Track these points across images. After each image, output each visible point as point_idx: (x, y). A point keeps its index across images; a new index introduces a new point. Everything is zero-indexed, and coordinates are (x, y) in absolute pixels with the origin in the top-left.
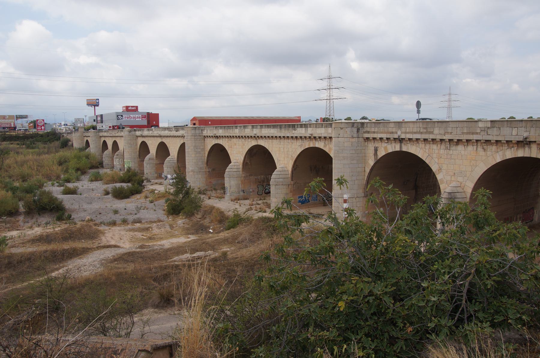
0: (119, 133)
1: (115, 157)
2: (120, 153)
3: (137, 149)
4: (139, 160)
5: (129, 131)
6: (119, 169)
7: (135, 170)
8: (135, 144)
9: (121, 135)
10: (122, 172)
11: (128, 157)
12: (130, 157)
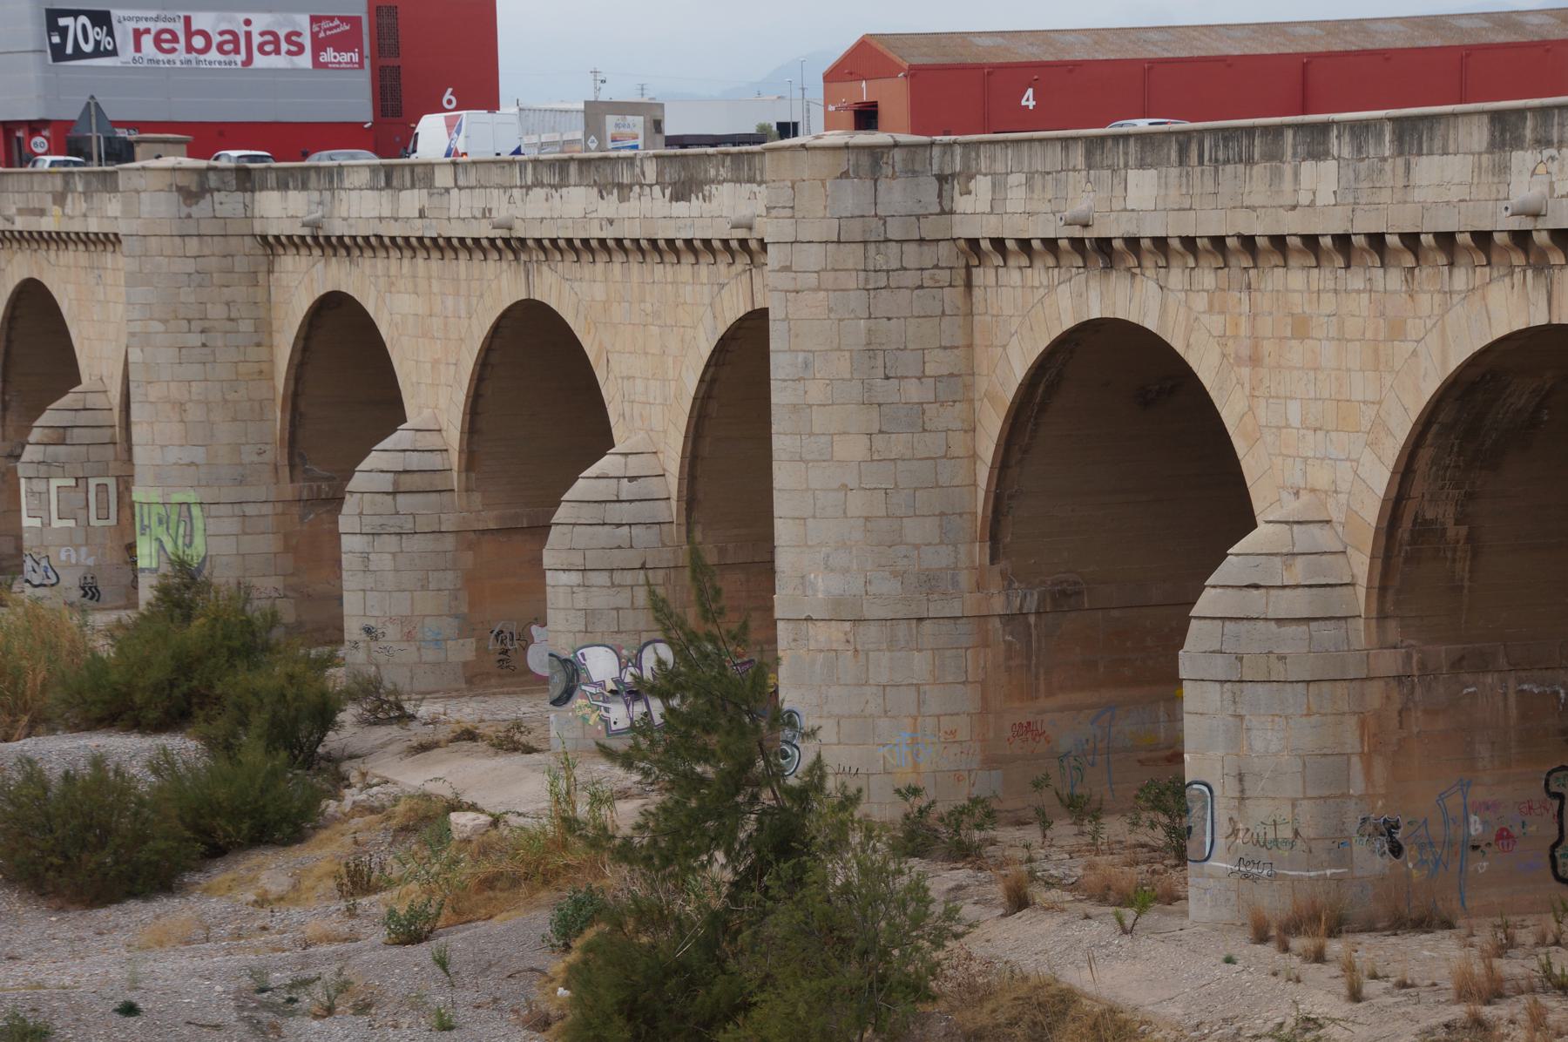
0: (75, 204)
1: (30, 453)
2: (83, 418)
3: (265, 375)
4: (288, 490)
5: (183, 180)
6: (71, 580)
7: (244, 591)
8: (246, 326)
9: (94, 226)
10: (101, 619)
11: (173, 455)
12: (199, 455)
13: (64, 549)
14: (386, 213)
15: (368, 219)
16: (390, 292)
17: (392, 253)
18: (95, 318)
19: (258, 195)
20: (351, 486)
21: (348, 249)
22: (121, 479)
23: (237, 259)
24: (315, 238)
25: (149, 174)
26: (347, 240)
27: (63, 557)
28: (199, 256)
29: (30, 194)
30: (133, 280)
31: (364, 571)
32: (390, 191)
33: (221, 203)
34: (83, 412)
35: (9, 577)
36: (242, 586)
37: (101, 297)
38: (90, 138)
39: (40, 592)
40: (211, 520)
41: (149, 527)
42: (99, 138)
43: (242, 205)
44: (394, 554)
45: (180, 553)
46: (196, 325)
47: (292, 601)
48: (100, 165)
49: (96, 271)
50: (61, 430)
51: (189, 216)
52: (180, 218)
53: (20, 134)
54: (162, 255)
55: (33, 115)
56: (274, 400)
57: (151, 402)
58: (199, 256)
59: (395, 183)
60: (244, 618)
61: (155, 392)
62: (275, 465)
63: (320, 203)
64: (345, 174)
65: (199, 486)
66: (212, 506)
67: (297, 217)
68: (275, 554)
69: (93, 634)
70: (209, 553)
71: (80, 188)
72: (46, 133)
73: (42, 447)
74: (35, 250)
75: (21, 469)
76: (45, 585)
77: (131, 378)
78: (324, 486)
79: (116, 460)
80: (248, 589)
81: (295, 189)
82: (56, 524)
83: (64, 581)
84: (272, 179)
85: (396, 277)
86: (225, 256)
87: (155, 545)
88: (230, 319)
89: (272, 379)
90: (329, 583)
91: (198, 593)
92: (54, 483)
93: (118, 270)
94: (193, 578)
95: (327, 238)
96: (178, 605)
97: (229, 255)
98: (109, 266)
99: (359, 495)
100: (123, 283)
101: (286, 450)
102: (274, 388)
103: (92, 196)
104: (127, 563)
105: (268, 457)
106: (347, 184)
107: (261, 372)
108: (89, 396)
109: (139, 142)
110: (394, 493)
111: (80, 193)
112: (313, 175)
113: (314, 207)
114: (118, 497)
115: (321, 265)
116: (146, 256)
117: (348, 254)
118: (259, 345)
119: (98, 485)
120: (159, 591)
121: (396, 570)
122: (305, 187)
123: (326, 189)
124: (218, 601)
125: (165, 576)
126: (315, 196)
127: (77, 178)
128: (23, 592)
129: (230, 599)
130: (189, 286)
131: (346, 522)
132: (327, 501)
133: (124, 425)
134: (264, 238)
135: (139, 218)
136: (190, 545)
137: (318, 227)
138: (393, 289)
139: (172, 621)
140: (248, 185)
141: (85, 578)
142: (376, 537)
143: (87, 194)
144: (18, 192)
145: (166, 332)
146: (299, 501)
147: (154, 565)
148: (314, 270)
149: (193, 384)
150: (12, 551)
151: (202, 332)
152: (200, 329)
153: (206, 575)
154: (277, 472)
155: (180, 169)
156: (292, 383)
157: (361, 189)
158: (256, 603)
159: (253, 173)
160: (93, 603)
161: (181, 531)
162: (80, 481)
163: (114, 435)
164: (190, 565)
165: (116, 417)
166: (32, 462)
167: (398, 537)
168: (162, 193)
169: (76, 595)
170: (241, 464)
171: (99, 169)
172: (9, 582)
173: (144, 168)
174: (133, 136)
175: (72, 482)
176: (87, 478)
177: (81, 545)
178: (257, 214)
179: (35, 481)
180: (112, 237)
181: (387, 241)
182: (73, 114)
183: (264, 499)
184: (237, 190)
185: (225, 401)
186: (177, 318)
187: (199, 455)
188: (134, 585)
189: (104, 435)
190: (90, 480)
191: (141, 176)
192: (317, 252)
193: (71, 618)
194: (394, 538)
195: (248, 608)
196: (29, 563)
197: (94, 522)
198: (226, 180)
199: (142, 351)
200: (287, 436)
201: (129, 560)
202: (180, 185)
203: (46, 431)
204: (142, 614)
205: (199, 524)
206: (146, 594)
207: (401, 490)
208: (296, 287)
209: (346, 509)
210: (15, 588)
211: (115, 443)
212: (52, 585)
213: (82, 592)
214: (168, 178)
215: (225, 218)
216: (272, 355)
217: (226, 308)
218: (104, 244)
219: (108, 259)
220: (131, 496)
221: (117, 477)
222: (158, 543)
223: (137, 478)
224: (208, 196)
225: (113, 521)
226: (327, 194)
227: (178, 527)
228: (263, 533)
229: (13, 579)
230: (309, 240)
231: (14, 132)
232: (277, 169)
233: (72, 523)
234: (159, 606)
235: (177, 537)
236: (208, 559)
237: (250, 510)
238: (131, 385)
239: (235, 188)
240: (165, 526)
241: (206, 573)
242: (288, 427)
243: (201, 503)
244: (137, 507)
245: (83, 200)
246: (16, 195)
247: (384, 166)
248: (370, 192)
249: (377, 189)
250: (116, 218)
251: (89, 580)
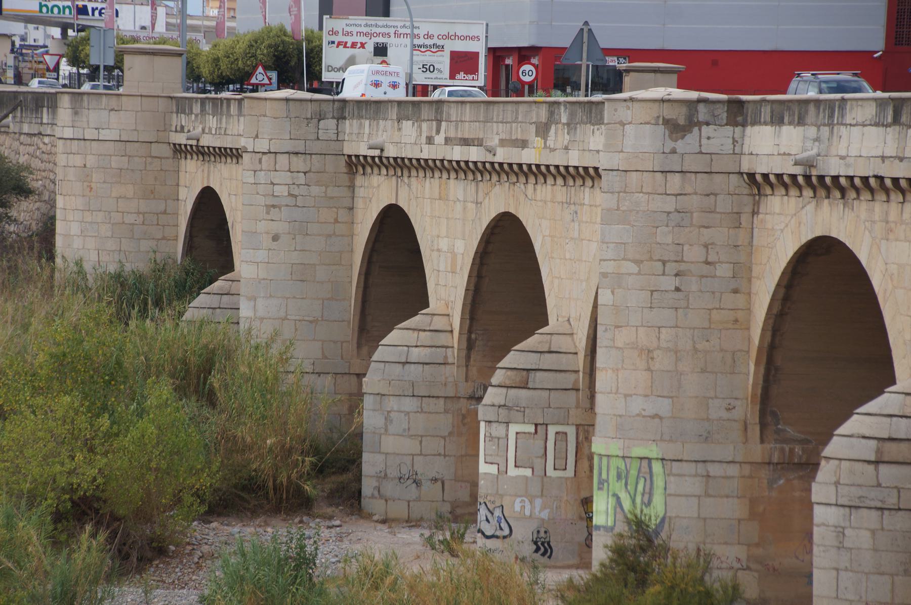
0: (558, 136)
1: (492, 396)
2: (548, 361)
3: (741, 324)
4: (757, 451)
5: (669, 112)
6: (523, 533)
7: (704, 559)
8: (724, 270)
9: (574, 158)
10: (552, 578)
11: (638, 405)
12: (664, 407)
13: (518, 500)
14: (890, 151)
15: (869, 158)
16: (887, 240)
17: (893, 196)
18: (568, 256)
19: (749, 130)
20: (828, 451)
21: (843, 191)
22: (581, 428)
23: (720, 197)
24: (808, 178)
25: (636, 105)
26: (843, 181)
27: (517, 508)
28: (681, 194)
29: (514, 125)
30: (610, 217)
31: (839, 548)
32: (897, 128)
33: (709, 138)
34: (547, 355)
35: (463, 525)
36: (702, 553)
37: (576, 235)
38: (581, 65)
39: (490, 544)
40: (672, 479)
41: (607, 481)
42: (588, 66)
43: (731, 141)
44: (873, 532)
45: (638, 512)
46: (671, 268)
47: (756, 575)
48: (586, 96)
49: (572, 207)
50: (525, 373)
51: (674, 151)
52: (664, 153)
53: (509, 61)
54: (641, 192)
55: (523, 41)
56: (748, 352)
57: (617, 348)
58: (681, 194)
59: (904, 119)
60: (702, 589)
61: (623, 337)
62: (745, 423)
63: (817, 139)
64: (848, 107)
65: (662, 440)
66: (674, 463)
67: (789, 154)
68: (739, 521)
69: (543, 593)
70: (668, 514)
71: (564, 119)
72: (535, 61)
73: (504, 390)
74: (514, 184)
75: (483, 412)
76: (497, 537)
77: (598, 322)
78: (798, 450)
79: (577, 407)
80: (709, 557)
81: (790, 124)
82: (513, 472)
83: (518, 534)
84: (766, 112)
85: (896, 223)
86: (708, 195)
87: (612, 501)
88: (707, 263)
89: (748, 329)
90: (797, 558)
91: (654, 557)
92: (514, 429)
93: (596, 206)
94: (650, 541)
95: (821, 178)
96: (632, 568)
97: (712, 194)
98: (586, 201)
99: (837, 462)
100: (599, 219)
101: (758, 407)
102: (749, 339)
103: (576, 129)
104: (581, 518)
105: (738, 413)
106: (848, 119)
107: (736, 321)
108: (555, 337)
109: (628, 71)
110: (877, 463)
111: (564, 124)
112: (812, 108)
113: (809, 144)
114: (577, 447)
115: (811, 207)
116: (625, 192)
117: (843, 196)
118: (736, 291)
119: (557, 433)
120: (613, 552)
121: (875, 550)
122: (801, 122)
123: (824, 125)
124: (675, 567)
125: (621, 536)
126: (812, 131)
127: (562, 108)
128: (475, 542)
129: (689, 566)
130: (667, 226)
131: (821, 490)
132: (800, 465)
133: (588, 370)
134: (752, 176)
135: (622, 151)
136: (649, 504)
137: (811, 166)
138: (891, 236)
139: (626, 586)
140: (740, 119)
141: (538, 532)
142: (853, 510)
143: (571, 126)
144: (502, 122)
145: (639, 273)
146: (769, 463)
147: (610, 523)
148: (804, 211)
149: (663, 330)
150: (467, 499)
151: (676, 275)
152: (675, 272)
153: (664, 537)
154: (746, 429)
155: (669, 101)
156: (769, 334)
157: (864, 126)
158: (716, 573)
159: (746, 106)
160: (544, 560)
161: (640, 487)
162: (539, 427)
163: (577, 381)
164: (648, 526)
165: (580, 362)
166: (493, 405)
167: (879, 513)
168: (648, 126)
169: (528, 549)
170: (708, 419)
171: (586, 99)
172: (462, 531)
173: (632, 99)
174: (623, 65)
175: (531, 429)
176: (547, 425)
177: (538, 497)
178: (746, 150)
179: (494, 425)
180: (591, 171)
181: (888, 183)
182: (564, 40)
183: (730, 459)
184: (726, 125)
185: (696, 350)
186: (651, 259)
187: (664, 407)
188: (588, 543)
189: (567, 380)
190: (550, 427)
191: (628, 108)
192: (808, 193)
193: (522, 575)
194: (875, 514)
195: (707, 578)
196: (483, 513)
197: (550, 472)
198: (716, 113)
199: (613, 293)
200: (759, 391)
201: (584, 515)
202: (666, 117)
203: (509, 373)
204: (595, 576)
205: (659, 482)
206: (600, 554)
207: (886, 459)
208: (782, 231)
209: (820, 476)
210: (468, 538)
211: (578, 390)
212: (505, 537)
213: (535, 547)
214: (655, 110)
215: (711, 154)
216: (750, 304)
217: (704, 250)
218: (583, 179)
219: (587, 195)
220: (590, 447)
221: (578, 426)
222: (615, 499)
223: (597, 427)
224: (696, 130)
225: (570, 472)
226: (825, 130)
227: (637, 483)
228: (727, 497)
229: (466, 528)
230: (800, 179)
231: (504, 60)
232: (773, 102)
233: (528, 472)
234: (612, 568)
235: (635, 495)
236: (667, 520)
237: (715, 470)
238: (599, 328)
239: (725, 121)
240: (624, 481)
241: (663, 535)
242: (761, 382)
243: (663, 459)
244: (596, 459)
245: (566, 131)
246: (501, 125)
247: (892, 99)
248: (874, 128)
249: (883, 125)
250: (598, 151)
251: (542, 534)
